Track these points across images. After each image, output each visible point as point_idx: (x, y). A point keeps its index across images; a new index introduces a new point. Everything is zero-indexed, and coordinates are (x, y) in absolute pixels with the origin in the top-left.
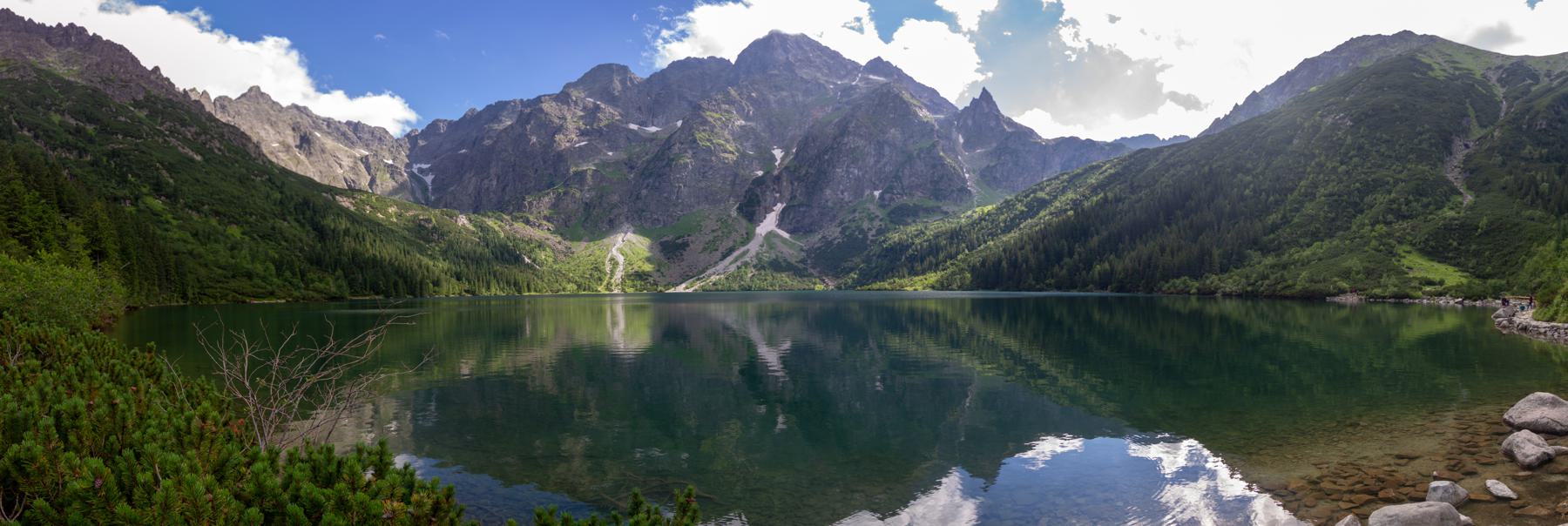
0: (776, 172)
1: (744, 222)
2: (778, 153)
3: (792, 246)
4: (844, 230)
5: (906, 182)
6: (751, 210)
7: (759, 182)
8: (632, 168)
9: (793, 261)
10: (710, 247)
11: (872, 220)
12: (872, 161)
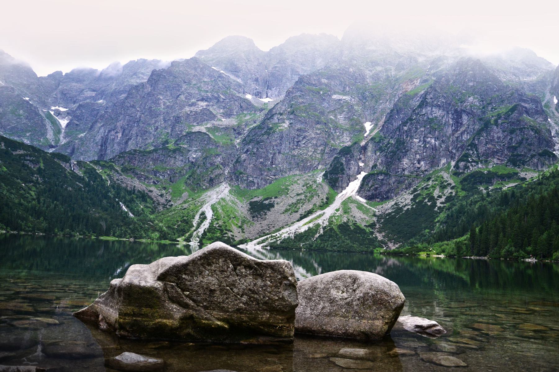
0: (363, 143)
1: (327, 188)
2: (368, 126)
3: (365, 211)
4: (416, 197)
5: (482, 149)
6: (336, 178)
7: (346, 151)
8: (239, 134)
9: (362, 225)
10: (292, 208)
11: (443, 187)
12: (450, 131)
